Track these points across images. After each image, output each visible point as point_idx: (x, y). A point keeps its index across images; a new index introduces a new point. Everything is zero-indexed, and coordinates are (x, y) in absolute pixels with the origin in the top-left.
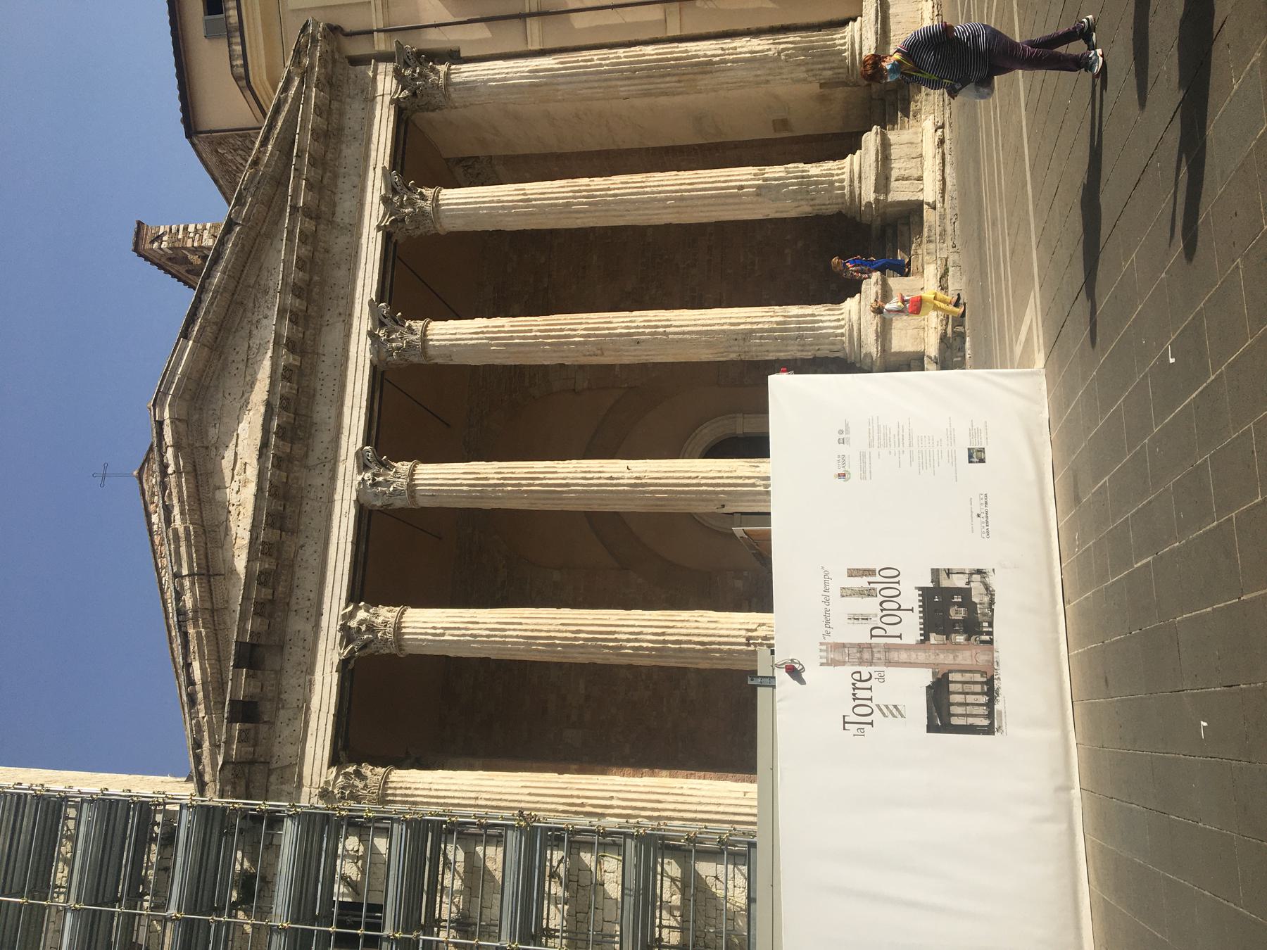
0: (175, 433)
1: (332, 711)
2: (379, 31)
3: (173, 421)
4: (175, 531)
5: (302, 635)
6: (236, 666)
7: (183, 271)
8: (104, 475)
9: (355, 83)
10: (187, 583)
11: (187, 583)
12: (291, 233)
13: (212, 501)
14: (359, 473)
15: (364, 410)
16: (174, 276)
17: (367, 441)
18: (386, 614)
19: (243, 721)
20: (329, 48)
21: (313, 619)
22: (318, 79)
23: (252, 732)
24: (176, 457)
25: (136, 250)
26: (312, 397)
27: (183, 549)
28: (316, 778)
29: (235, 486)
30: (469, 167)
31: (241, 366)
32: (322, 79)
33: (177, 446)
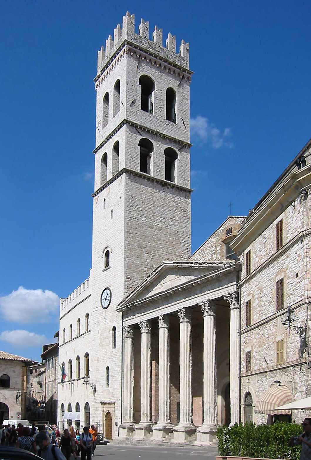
4: (147, 280)
10: (141, 286)
11: (141, 286)
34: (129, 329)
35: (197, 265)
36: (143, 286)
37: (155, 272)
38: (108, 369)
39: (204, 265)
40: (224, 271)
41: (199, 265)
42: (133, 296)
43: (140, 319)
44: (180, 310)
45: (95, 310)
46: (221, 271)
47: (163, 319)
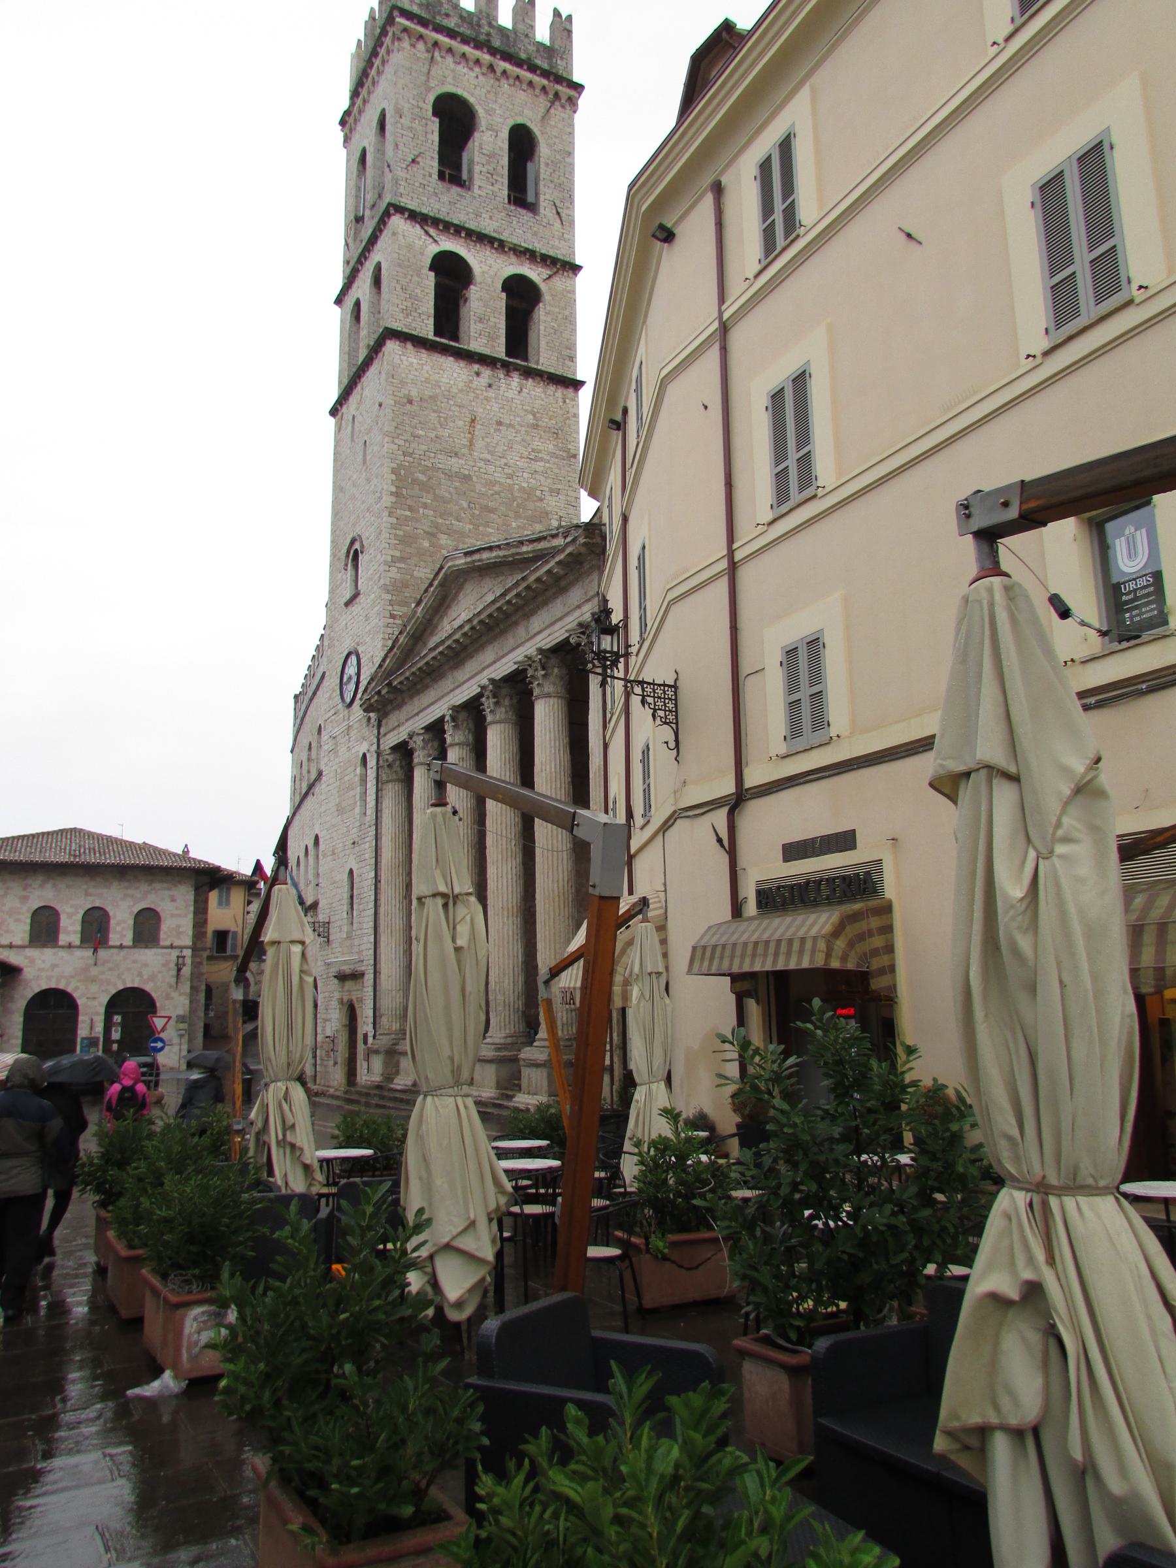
13: (442, 617)
33: (441, 585)
34: (390, 758)
38: (351, 872)
39: (524, 549)
40: (562, 556)
43: (409, 724)
44: (483, 688)
45: (330, 714)
46: (557, 559)
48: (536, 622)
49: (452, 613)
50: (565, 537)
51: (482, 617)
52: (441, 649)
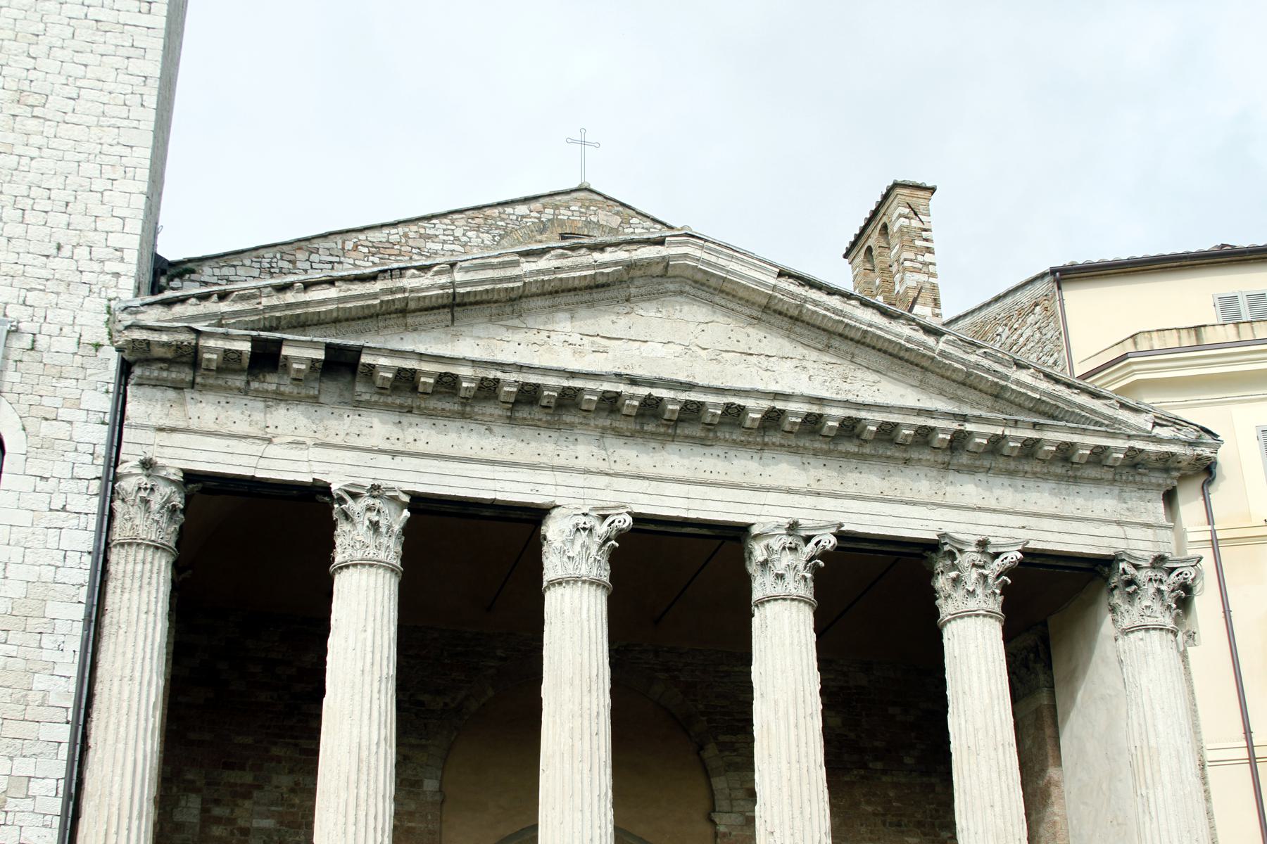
0: (649, 263)
1: (260, 474)
2: (1213, 532)
3: (665, 261)
4: (515, 264)
5: (366, 431)
6: (329, 347)
7: (871, 242)
8: (583, 143)
9: (1141, 499)
10: (444, 279)
11: (444, 279)
12: (930, 413)
13: (554, 308)
14: (596, 509)
15: (684, 514)
16: (863, 230)
17: (638, 518)
18: (390, 550)
19: (254, 354)
20: (1184, 464)
21: (387, 446)
22: (1142, 451)
23: (236, 366)
24: (616, 263)
25: (896, 185)
26: (703, 442)
27: (490, 274)
28: (168, 452)
29: (575, 339)
30: (1037, 654)
31: (743, 347)
32: (1140, 457)
33: (630, 266)
35: (973, 358)
36: (464, 284)
37: (597, 256)
39: (1024, 376)
40: (1151, 447)
41: (986, 363)
42: (339, 300)
46: (1139, 445)
47: (621, 536)
48: (968, 490)
49: (608, 322)
50: (1155, 424)
51: (863, 414)
52: (658, 392)
